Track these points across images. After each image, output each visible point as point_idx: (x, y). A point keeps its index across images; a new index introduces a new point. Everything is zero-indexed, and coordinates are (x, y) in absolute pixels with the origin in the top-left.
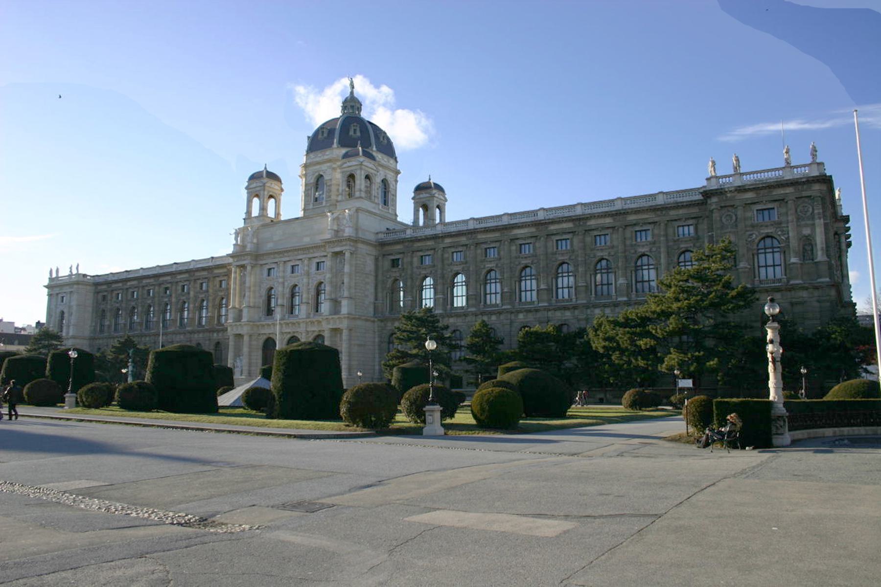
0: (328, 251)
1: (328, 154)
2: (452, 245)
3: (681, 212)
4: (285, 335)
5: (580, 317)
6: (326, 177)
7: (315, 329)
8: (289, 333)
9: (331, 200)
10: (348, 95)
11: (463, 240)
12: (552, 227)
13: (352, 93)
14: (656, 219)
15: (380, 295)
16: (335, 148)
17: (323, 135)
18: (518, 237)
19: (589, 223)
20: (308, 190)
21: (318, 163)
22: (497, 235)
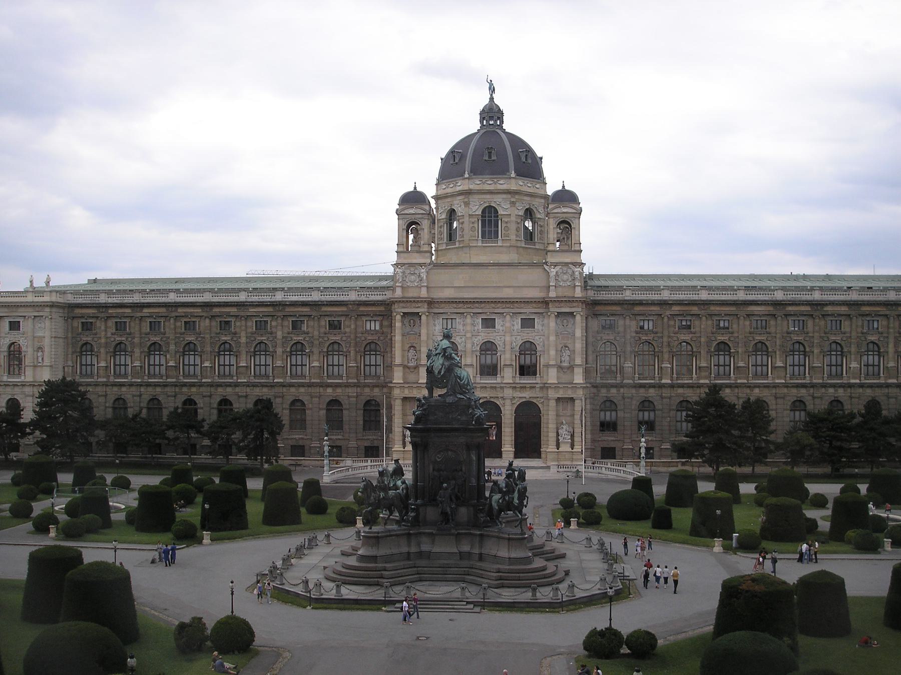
0: (551, 310)
1: (503, 184)
5: (815, 395)
6: (501, 212)
7: (527, 395)
10: (487, 101)
11: (695, 310)
12: (790, 308)
13: (492, 99)
14: (888, 313)
15: (590, 358)
16: (513, 178)
17: (490, 157)
19: (825, 309)
20: (473, 223)
21: (491, 192)
22: (733, 308)
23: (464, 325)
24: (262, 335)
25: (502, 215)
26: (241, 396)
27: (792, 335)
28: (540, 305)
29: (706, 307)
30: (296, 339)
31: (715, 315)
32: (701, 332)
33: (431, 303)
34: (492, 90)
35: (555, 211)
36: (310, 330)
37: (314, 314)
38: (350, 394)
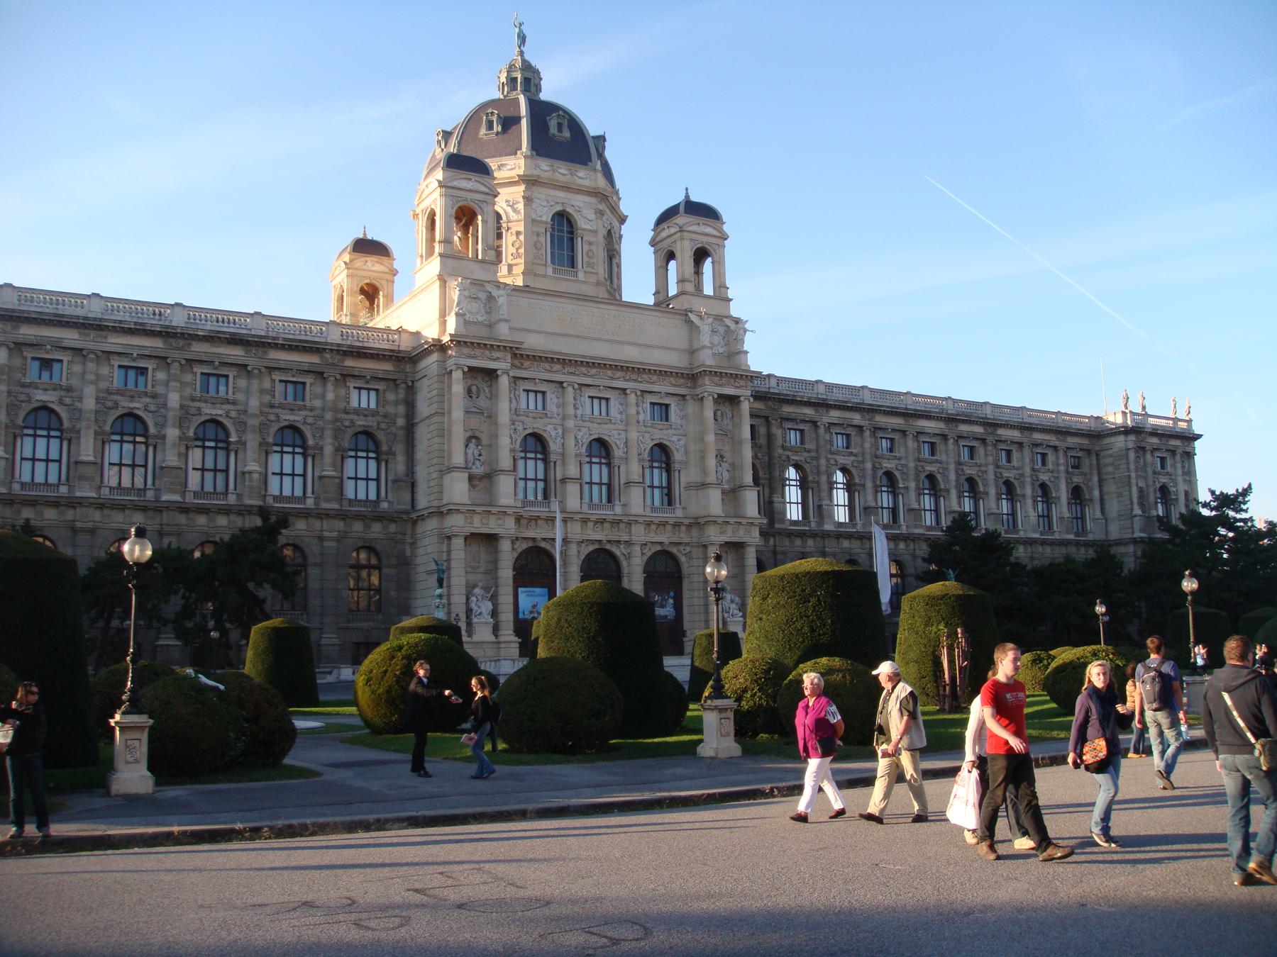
2: (841, 422)
3: (1076, 440)
4: (583, 545)
6: (581, 223)
7: (665, 537)
8: (600, 541)
9: (597, 274)
11: (857, 418)
12: (964, 428)
14: (1057, 443)
18: (927, 431)
23: (558, 406)
24: (132, 397)
25: (584, 230)
26: (84, 530)
27: (965, 468)
28: (682, 381)
29: (870, 414)
30: (209, 411)
31: (880, 429)
32: (863, 455)
33: (518, 355)
34: (522, 39)
35: (691, 228)
36: (240, 397)
37: (252, 362)
38: (326, 534)
